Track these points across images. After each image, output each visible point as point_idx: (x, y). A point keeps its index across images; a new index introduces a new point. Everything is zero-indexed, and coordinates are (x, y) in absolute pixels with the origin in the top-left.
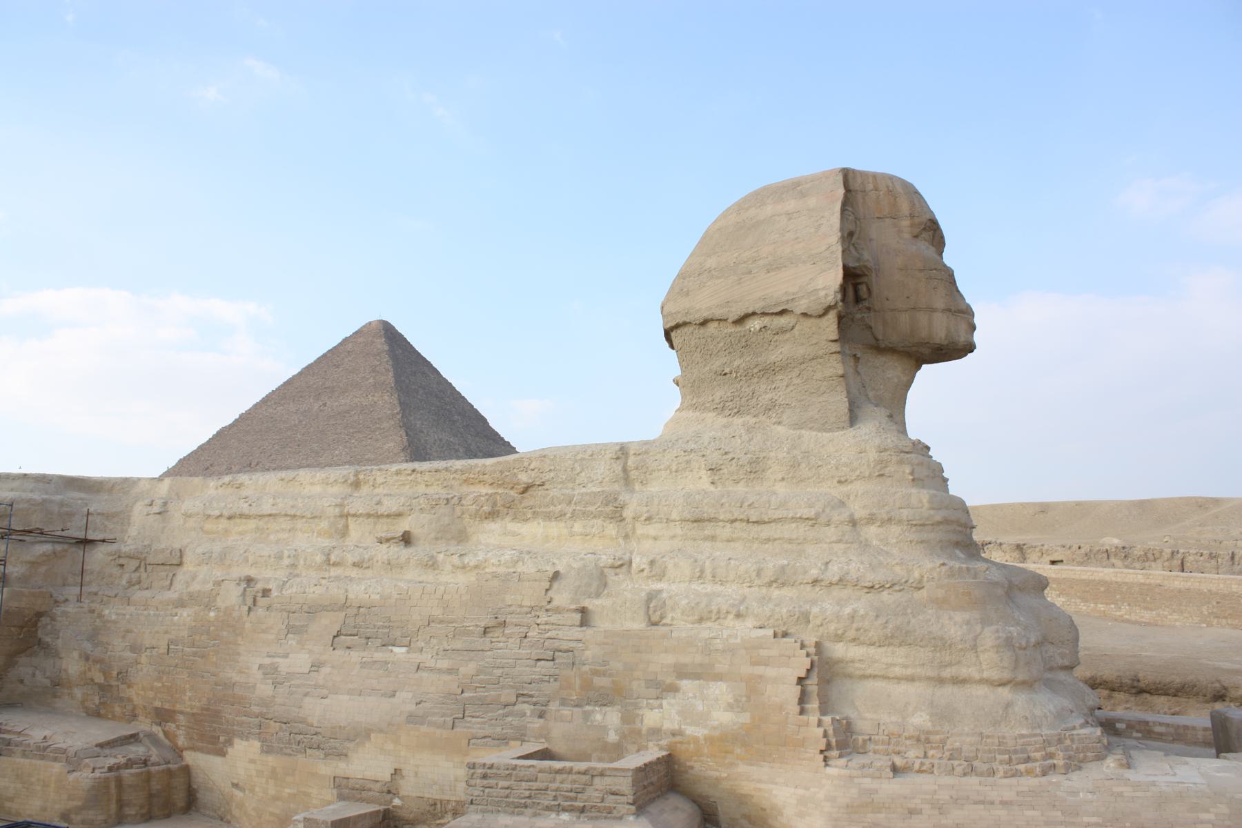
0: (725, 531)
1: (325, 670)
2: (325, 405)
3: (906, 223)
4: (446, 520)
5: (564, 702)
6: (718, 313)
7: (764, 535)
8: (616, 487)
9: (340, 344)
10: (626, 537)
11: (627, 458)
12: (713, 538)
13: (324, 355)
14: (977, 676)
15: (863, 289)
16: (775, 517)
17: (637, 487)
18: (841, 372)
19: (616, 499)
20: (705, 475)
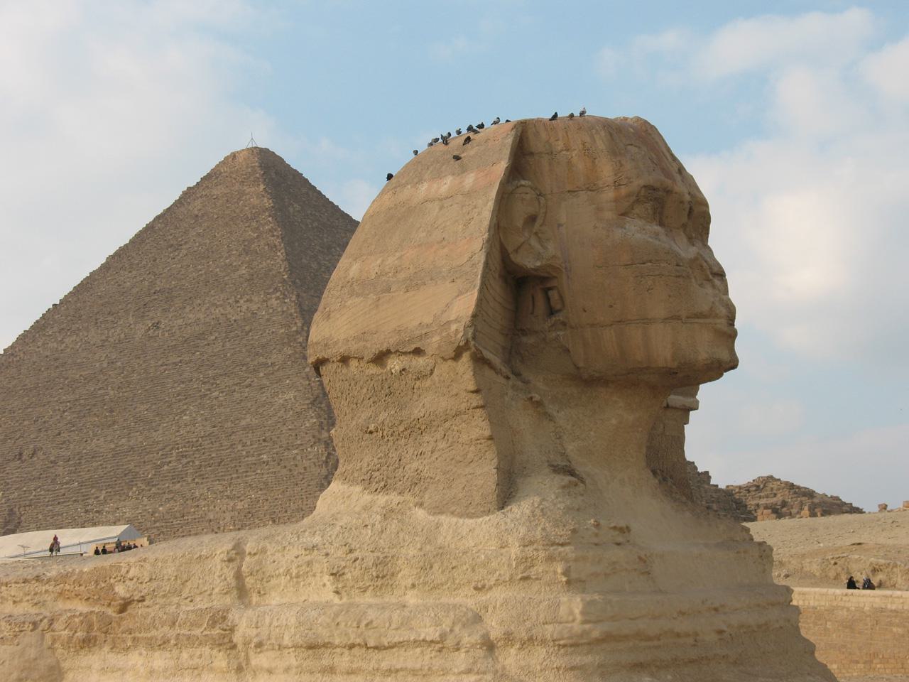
0: (343, 660)
2: (156, 326)
4: (32, 653)
6: (354, 347)
7: (384, 665)
8: (228, 600)
9: (178, 203)
10: (240, 669)
11: (243, 559)
12: (331, 670)
13: (150, 228)
15: (554, 295)
16: (396, 640)
17: (255, 598)
18: (487, 433)
19: (224, 618)
20: (327, 579)
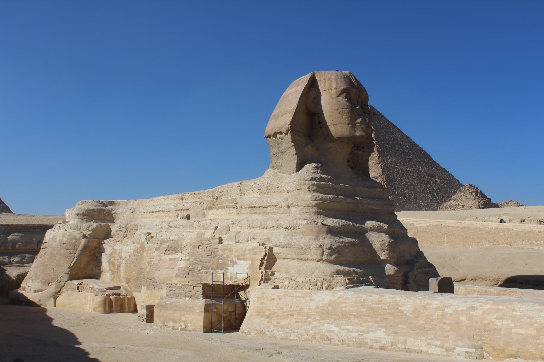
0: (258, 210)
1: (161, 262)
3: (334, 91)
5: (212, 269)
12: (256, 213)
14: (310, 258)
17: (243, 196)
